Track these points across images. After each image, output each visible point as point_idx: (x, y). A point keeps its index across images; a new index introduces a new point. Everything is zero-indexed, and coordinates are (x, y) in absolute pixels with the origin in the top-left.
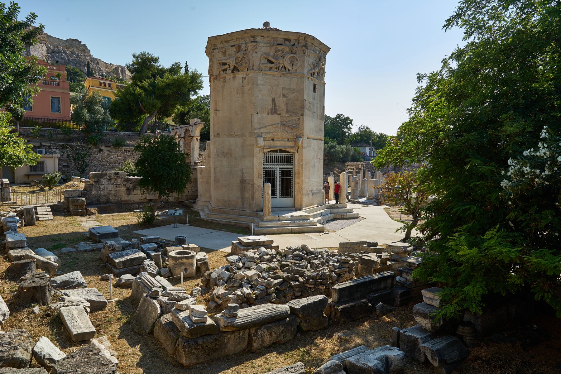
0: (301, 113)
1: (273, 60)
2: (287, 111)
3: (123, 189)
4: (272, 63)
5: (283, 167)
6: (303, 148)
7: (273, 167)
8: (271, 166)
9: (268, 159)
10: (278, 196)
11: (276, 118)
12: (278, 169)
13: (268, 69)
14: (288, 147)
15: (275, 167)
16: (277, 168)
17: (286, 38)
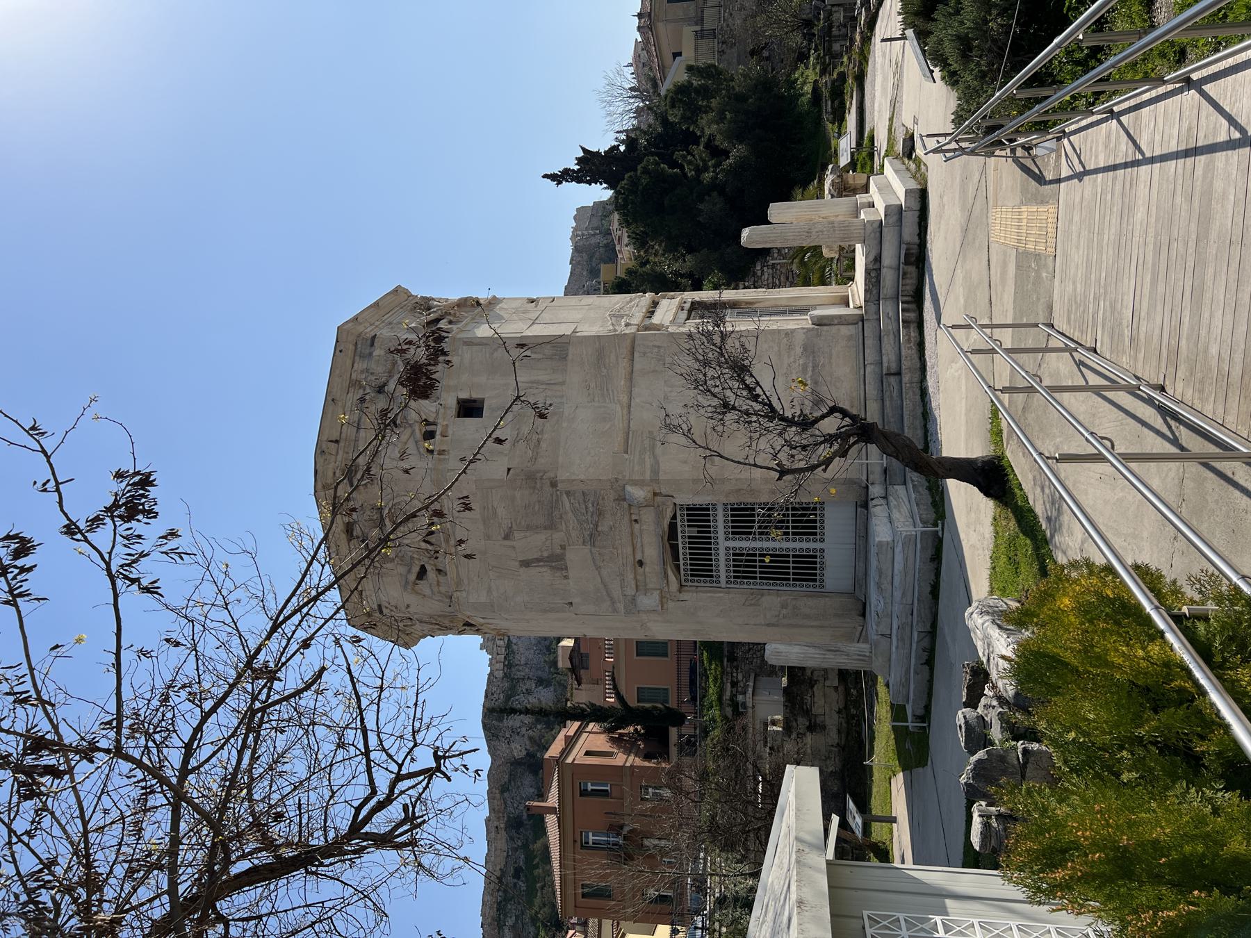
0: (548, 489)
1: (416, 569)
2: (551, 526)
3: (809, 739)
4: (422, 573)
5: (721, 530)
6: (657, 481)
7: (722, 558)
8: (722, 563)
9: (702, 569)
10: (818, 545)
11: (577, 556)
12: (731, 544)
13: (441, 578)
14: (658, 523)
15: (722, 552)
16: (727, 548)
17: (344, 536)
